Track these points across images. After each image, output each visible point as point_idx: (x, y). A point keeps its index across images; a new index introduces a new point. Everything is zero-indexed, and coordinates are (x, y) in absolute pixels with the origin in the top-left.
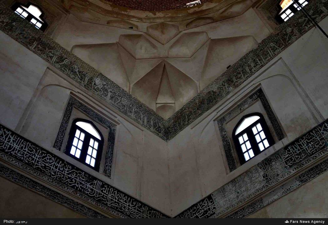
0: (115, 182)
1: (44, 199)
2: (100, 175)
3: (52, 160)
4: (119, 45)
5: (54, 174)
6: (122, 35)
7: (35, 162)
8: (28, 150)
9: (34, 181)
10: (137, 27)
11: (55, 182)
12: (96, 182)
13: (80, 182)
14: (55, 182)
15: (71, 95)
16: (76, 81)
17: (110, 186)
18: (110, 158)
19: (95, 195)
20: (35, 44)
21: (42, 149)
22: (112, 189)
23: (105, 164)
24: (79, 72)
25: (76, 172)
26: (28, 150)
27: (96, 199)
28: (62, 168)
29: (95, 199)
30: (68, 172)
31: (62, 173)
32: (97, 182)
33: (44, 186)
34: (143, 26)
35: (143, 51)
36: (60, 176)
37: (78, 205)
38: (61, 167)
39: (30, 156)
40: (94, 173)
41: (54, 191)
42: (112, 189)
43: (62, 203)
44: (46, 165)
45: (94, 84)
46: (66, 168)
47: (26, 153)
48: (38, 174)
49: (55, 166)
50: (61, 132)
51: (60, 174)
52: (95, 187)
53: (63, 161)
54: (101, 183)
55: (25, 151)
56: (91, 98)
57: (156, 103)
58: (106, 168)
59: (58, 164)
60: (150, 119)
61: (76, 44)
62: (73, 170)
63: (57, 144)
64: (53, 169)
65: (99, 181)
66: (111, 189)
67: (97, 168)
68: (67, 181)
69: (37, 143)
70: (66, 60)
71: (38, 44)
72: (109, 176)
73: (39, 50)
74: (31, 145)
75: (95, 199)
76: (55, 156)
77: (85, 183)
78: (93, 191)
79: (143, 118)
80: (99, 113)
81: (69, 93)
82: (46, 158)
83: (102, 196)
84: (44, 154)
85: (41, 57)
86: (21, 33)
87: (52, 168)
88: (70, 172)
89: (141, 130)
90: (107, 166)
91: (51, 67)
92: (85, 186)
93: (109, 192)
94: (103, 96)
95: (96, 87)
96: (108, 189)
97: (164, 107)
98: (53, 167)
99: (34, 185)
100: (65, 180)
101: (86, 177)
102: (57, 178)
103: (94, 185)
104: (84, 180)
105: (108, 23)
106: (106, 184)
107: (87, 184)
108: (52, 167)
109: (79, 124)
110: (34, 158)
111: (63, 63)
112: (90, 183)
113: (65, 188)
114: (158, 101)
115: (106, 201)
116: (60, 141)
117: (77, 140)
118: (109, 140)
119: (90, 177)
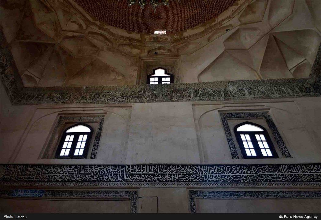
0: (297, 158)
1: (251, 200)
2: (282, 160)
3: (238, 169)
4: (227, 50)
5: (246, 179)
6: (225, 41)
7: (227, 178)
8: (218, 171)
9: (235, 192)
10: (231, 25)
11: (250, 184)
12: (282, 168)
13: (269, 174)
14: (250, 184)
15: (220, 112)
16: (216, 100)
17: (295, 165)
18: (280, 141)
19: (287, 178)
20: (174, 95)
21: (226, 165)
22: (299, 166)
23: (280, 148)
24: (214, 92)
25: (261, 169)
26: (218, 171)
27: (291, 181)
28: (249, 171)
29: (290, 182)
30: (255, 172)
31: (251, 175)
32: (283, 168)
33: (245, 192)
34: (235, 21)
35: (249, 40)
36: (251, 178)
37: (279, 193)
38: (248, 171)
39: (221, 175)
40: (275, 161)
41: (254, 192)
42: (299, 166)
43: (265, 197)
44: (236, 175)
45: (230, 92)
46: (252, 170)
47: (217, 174)
48: (235, 185)
49: (243, 172)
50: (230, 144)
51: (250, 177)
52: (283, 172)
53: (246, 166)
54: (286, 166)
55: (216, 173)
56: (234, 105)
57: (290, 70)
58: (282, 151)
59: (244, 170)
60: (293, 87)
61: (198, 75)
62: (258, 168)
63: (234, 155)
64: (243, 176)
65: (283, 166)
66: (298, 167)
67: (275, 155)
68: (259, 179)
69: (221, 163)
70: (200, 90)
71: (176, 94)
72: (290, 156)
73: (179, 97)
74: (217, 167)
75: (290, 182)
76: (238, 166)
77: (274, 173)
78: (284, 176)
79: (287, 90)
80: (248, 112)
81: (218, 112)
82: (233, 170)
83: (294, 176)
84: (230, 168)
85: (184, 101)
86: (163, 95)
87: (242, 175)
88: (256, 170)
89: (292, 101)
90: (282, 149)
91: (193, 103)
92: (275, 176)
93: (298, 170)
94: (242, 97)
95: (233, 94)
96: (296, 168)
97: (299, 68)
98: (242, 174)
99: (237, 194)
100: (257, 179)
101: (271, 168)
102: (249, 180)
103: (282, 171)
104: (271, 171)
105: (209, 40)
106: (291, 165)
107: (275, 173)
108: (241, 175)
109: (239, 129)
110: (225, 175)
111: (199, 94)
112: (277, 171)
113: (260, 185)
114: (290, 67)
115: (300, 179)
116: (234, 151)
117: (246, 142)
118: (270, 127)
119: (275, 166)
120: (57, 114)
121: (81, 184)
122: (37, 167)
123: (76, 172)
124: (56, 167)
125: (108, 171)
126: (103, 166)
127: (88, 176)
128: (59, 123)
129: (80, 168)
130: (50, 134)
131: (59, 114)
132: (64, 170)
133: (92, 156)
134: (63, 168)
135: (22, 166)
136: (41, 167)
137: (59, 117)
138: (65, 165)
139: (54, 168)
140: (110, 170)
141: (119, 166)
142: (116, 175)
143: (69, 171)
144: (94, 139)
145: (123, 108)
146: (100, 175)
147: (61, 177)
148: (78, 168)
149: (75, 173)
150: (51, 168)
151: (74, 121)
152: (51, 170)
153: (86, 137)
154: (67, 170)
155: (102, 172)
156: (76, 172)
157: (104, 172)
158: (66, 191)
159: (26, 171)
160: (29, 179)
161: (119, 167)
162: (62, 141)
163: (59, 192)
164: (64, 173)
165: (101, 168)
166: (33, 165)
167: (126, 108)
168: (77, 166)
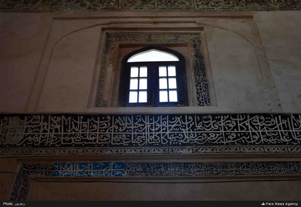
120: (99, 28)
121: (206, 149)
122: (97, 120)
123: (185, 128)
124: (140, 119)
125: (255, 126)
126: (241, 117)
127: (214, 135)
128: (108, 44)
129: (194, 121)
130: (96, 63)
131: (103, 29)
132: (159, 126)
133: (200, 103)
134: (155, 121)
135: (63, 117)
136: (106, 119)
137: (104, 35)
138: (160, 115)
139: (135, 121)
140: (259, 124)
141: (276, 115)
142: (275, 133)
143: (170, 128)
144: (193, 74)
145: (237, 20)
146: (240, 133)
147: (156, 138)
148: (188, 120)
149: (183, 130)
150: (128, 122)
151: (137, 43)
152: (128, 126)
153: (172, 71)
154: (164, 125)
155: (242, 129)
156: (185, 128)
157: (247, 127)
158: (174, 163)
159: (74, 127)
160: (85, 143)
161: (276, 118)
162: (126, 78)
163: (160, 167)
164: (159, 130)
165: (238, 120)
166: (86, 117)
167: (241, 20)
168: (186, 116)
